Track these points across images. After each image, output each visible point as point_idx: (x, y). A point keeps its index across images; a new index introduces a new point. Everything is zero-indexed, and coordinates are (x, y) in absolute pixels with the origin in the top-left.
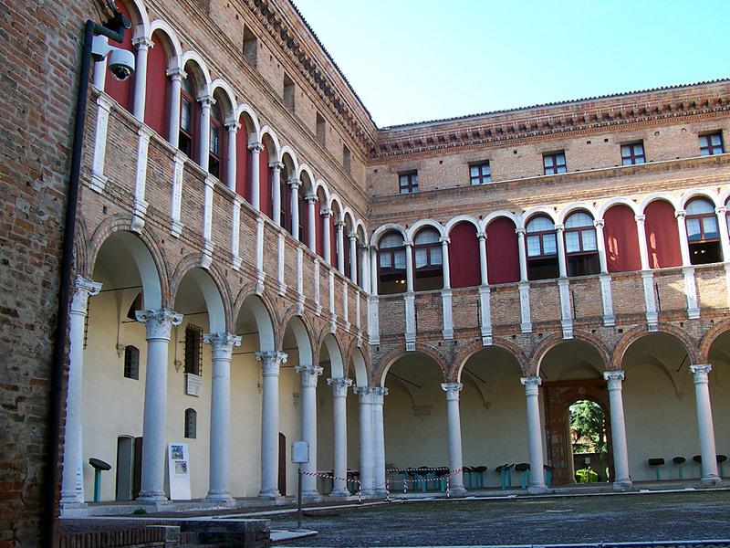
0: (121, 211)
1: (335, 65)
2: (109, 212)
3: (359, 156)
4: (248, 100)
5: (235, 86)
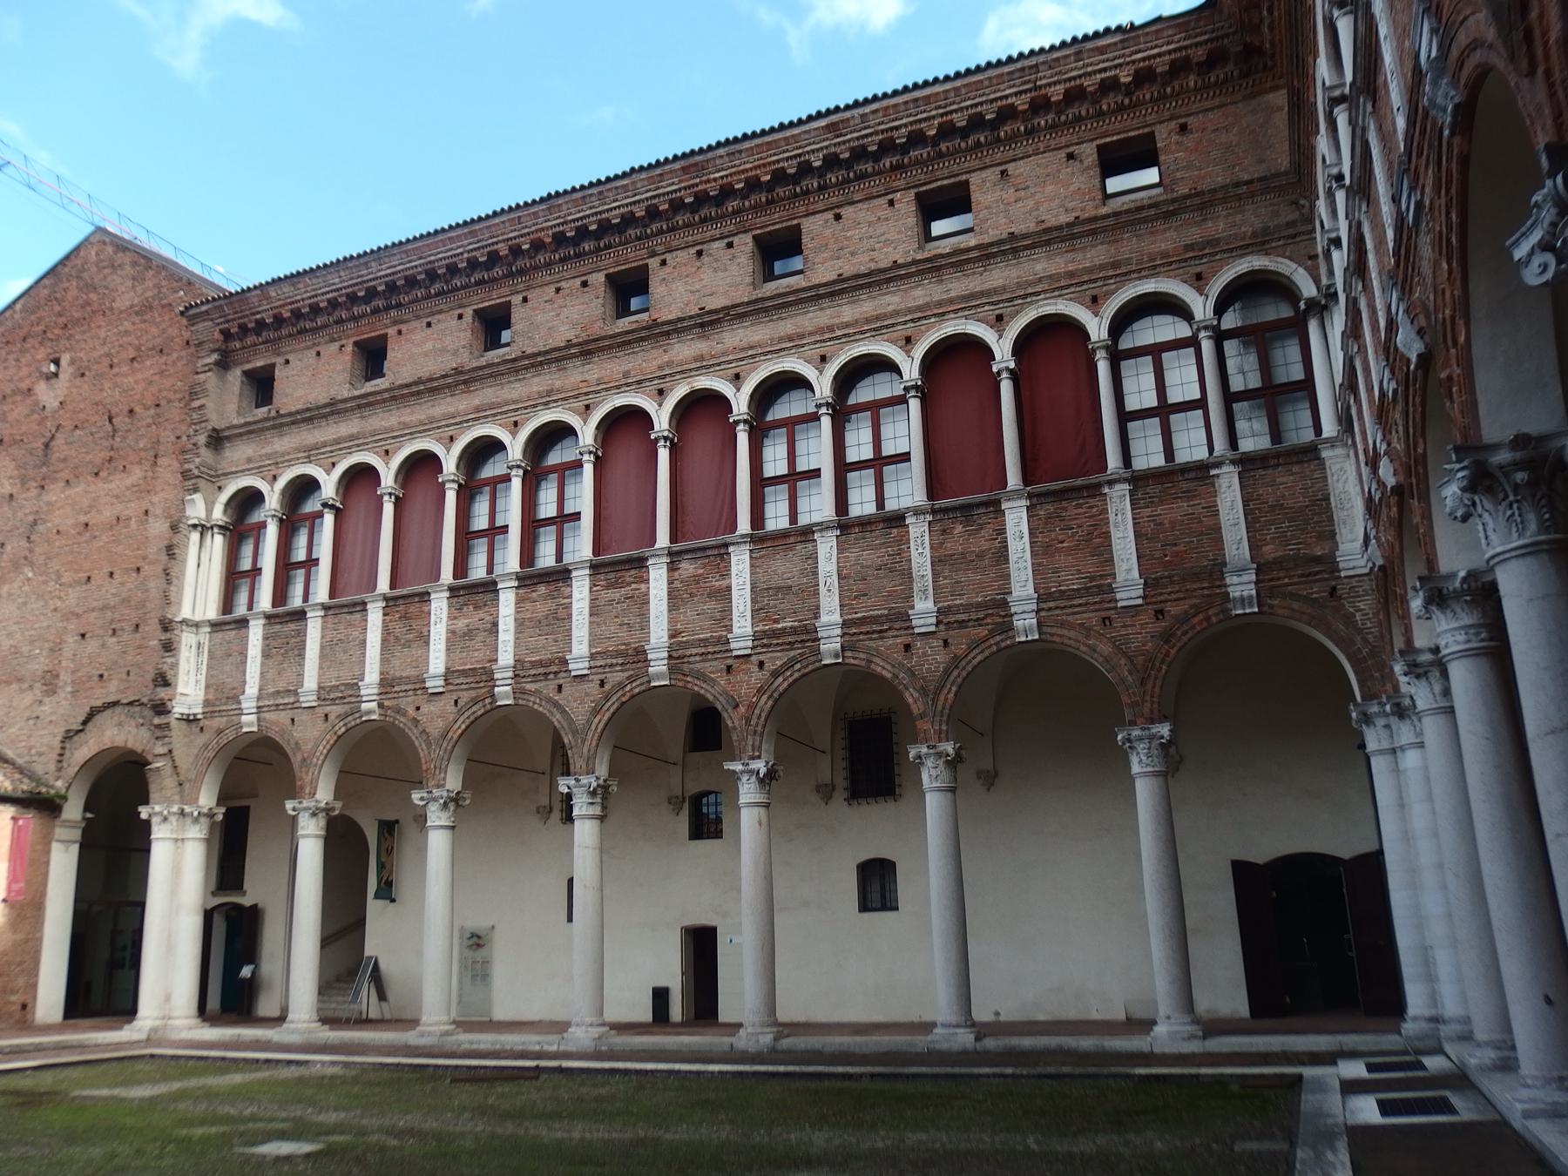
0: (347, 707)
1: (857, 104)
2: (332, 717)
3: (1208, 104)
4: (618, 387)
5: (575, 397)
